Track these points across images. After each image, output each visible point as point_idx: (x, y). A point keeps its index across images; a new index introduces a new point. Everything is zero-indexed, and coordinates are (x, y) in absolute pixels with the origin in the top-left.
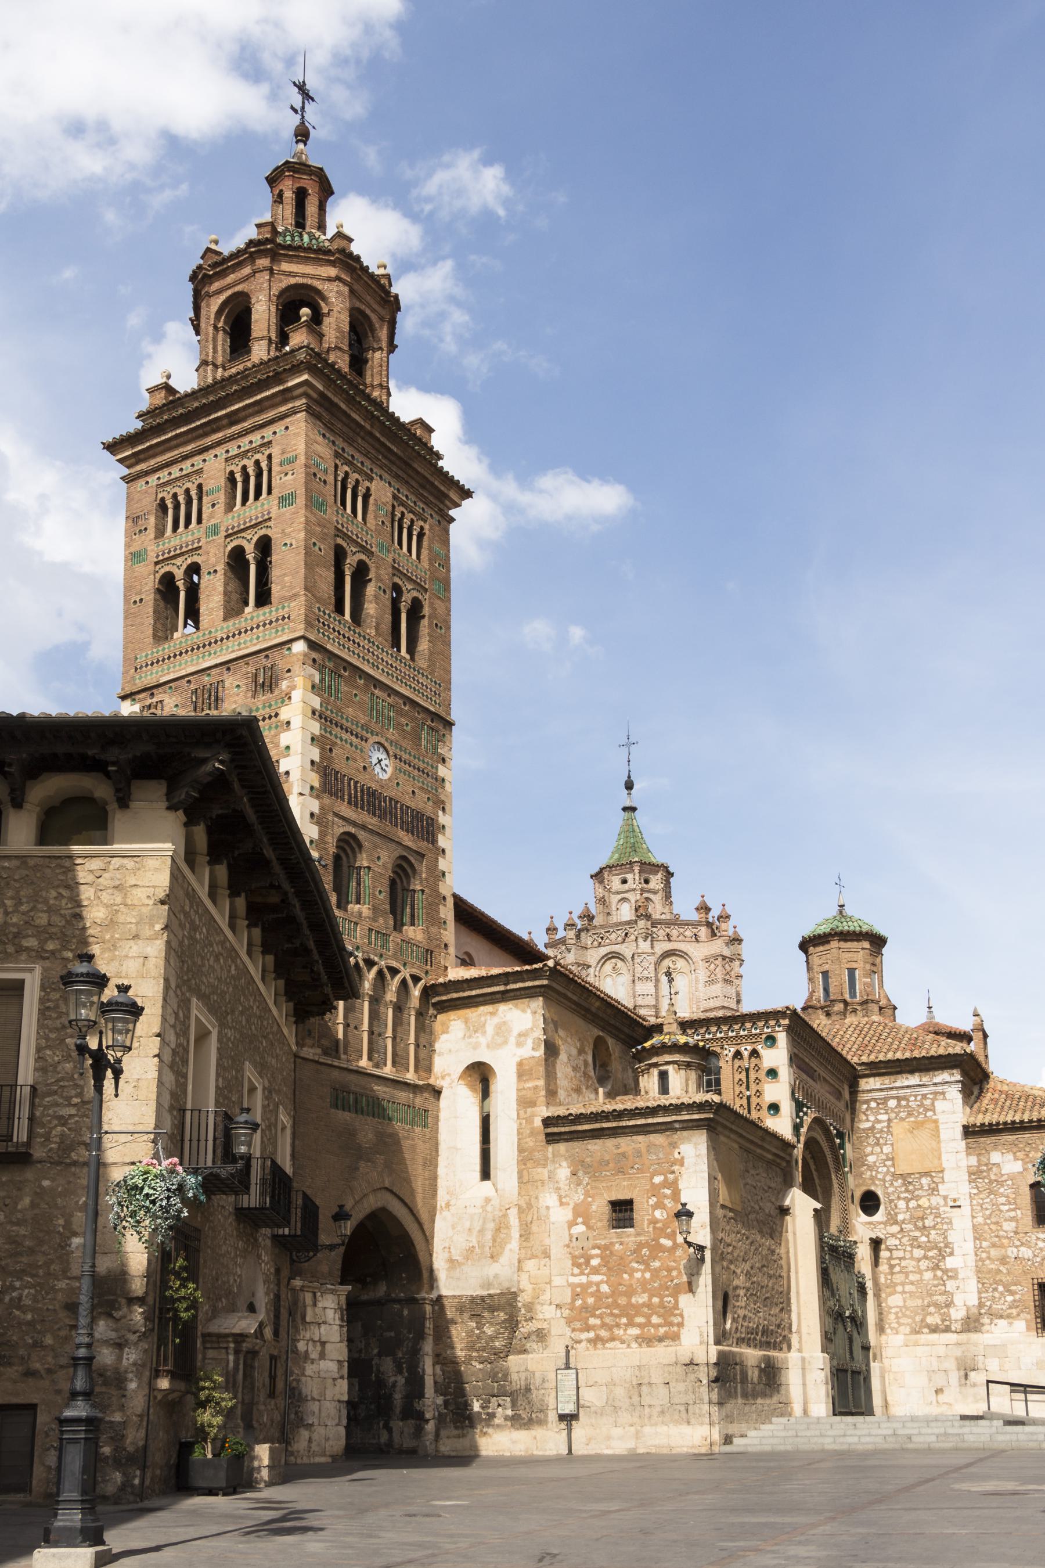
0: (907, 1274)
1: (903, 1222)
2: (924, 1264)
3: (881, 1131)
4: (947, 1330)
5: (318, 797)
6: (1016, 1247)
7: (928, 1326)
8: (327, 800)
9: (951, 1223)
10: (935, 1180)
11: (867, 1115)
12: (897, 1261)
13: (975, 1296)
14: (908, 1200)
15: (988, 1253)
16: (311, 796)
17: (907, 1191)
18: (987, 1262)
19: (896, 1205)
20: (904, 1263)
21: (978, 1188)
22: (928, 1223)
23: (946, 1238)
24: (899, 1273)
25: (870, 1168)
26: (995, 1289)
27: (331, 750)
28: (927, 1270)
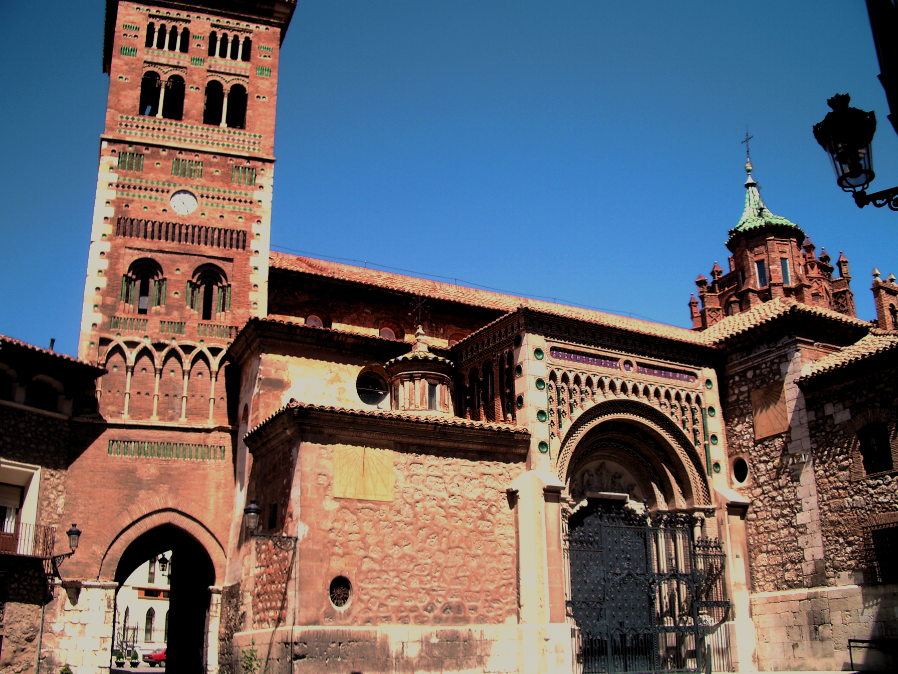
2: (782, 521)
3: (744, 402)
4: (800, 585)
5: (109, 240)
8: (120, 240)
15: (828, 505)
16: (102, 240)
17: (766, 454)
18: (829, 514)
19: (758, 470)
21: (817, 442)
26: (837, 541)
27: (127, 206)
28: (782, 529)
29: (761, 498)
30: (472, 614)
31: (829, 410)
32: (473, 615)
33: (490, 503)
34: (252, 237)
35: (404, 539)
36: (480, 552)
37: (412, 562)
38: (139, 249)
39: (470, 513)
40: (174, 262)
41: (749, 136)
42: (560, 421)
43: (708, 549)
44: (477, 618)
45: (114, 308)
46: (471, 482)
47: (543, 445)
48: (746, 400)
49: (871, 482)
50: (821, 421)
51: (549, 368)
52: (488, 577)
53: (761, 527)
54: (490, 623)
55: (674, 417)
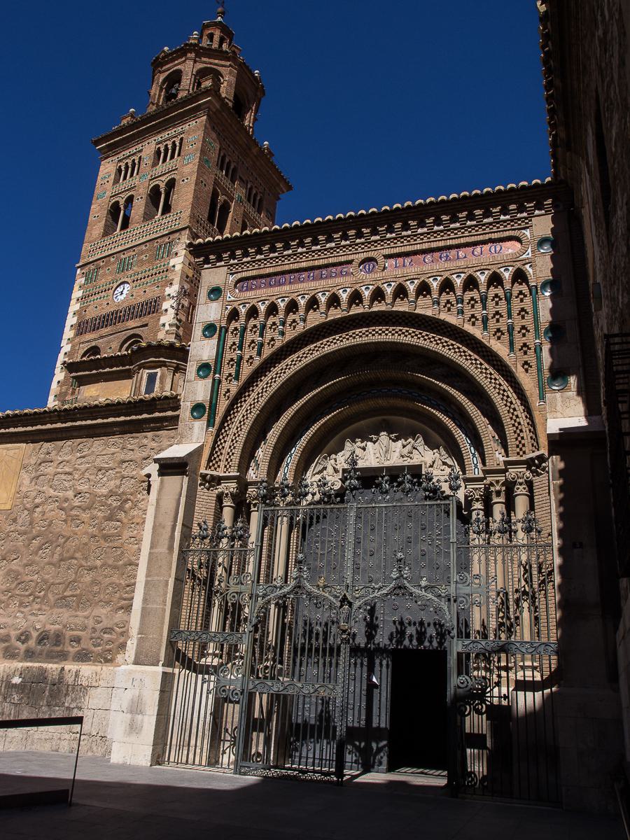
16: (67, 344)
27: (85, 311)
30: (73, 647)
32: (73, 649)
33: (125, 497)
34: (164, 300)
35: (14, 551)
36: (98, 563)
37: (16, 579)
38: (88, 342)
39: (95, 512)
40: (109, 342)
44: (78, 653)
45: (66, 394)
46: (108, 474)
47: (198, 408)
51: (229, 307)
52: (102, 597)
54: (94, 661)
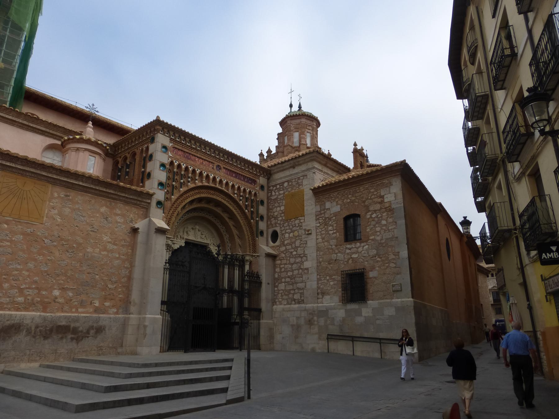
0: (287, 272)
1: (287, 245)
3: (281, 199)
6: (336, 254)
7: (294, 300)
9: (306, 243)
10: (302, 221)
11: (275, 192)
12: (283, 266)
13: (316, 282)
14: (289, 234)
20: (286, 266)
21: (319, 223)
22: (298, 243)
23: (304, 251)
24: (283, 272)
25: (276, 218)
29: (285, 252)
31: (328, 205)
41: (292, 90)
42: (173, 191)
43: (253, 278)
47: (159, 203)
48: (282, 198)
49: (348, 246)
50: (323, 212)
53: (283, 268)
55: (241, 202)
